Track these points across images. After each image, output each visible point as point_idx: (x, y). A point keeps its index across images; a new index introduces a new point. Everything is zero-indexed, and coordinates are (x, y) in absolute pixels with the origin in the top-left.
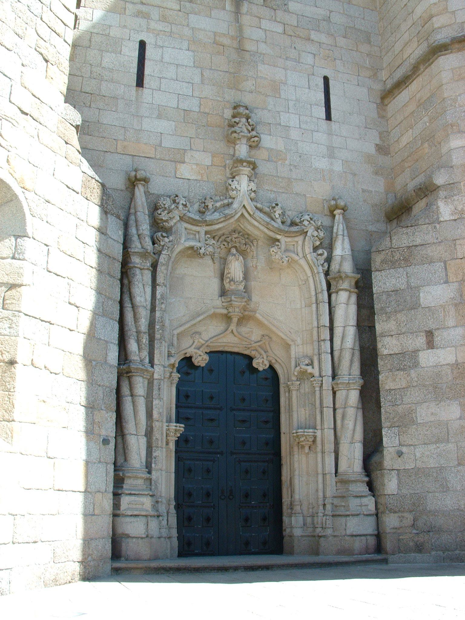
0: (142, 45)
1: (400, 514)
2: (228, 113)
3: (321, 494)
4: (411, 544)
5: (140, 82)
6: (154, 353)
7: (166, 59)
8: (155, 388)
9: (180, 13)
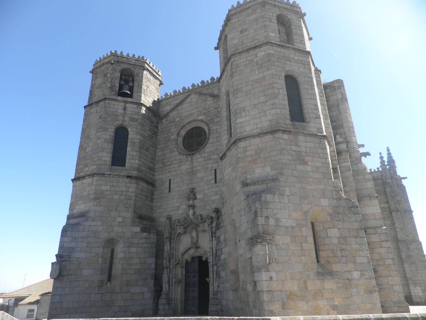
0: (170, 180)
5: (170, 191)
7: (175, 182)
9: (178, 167)
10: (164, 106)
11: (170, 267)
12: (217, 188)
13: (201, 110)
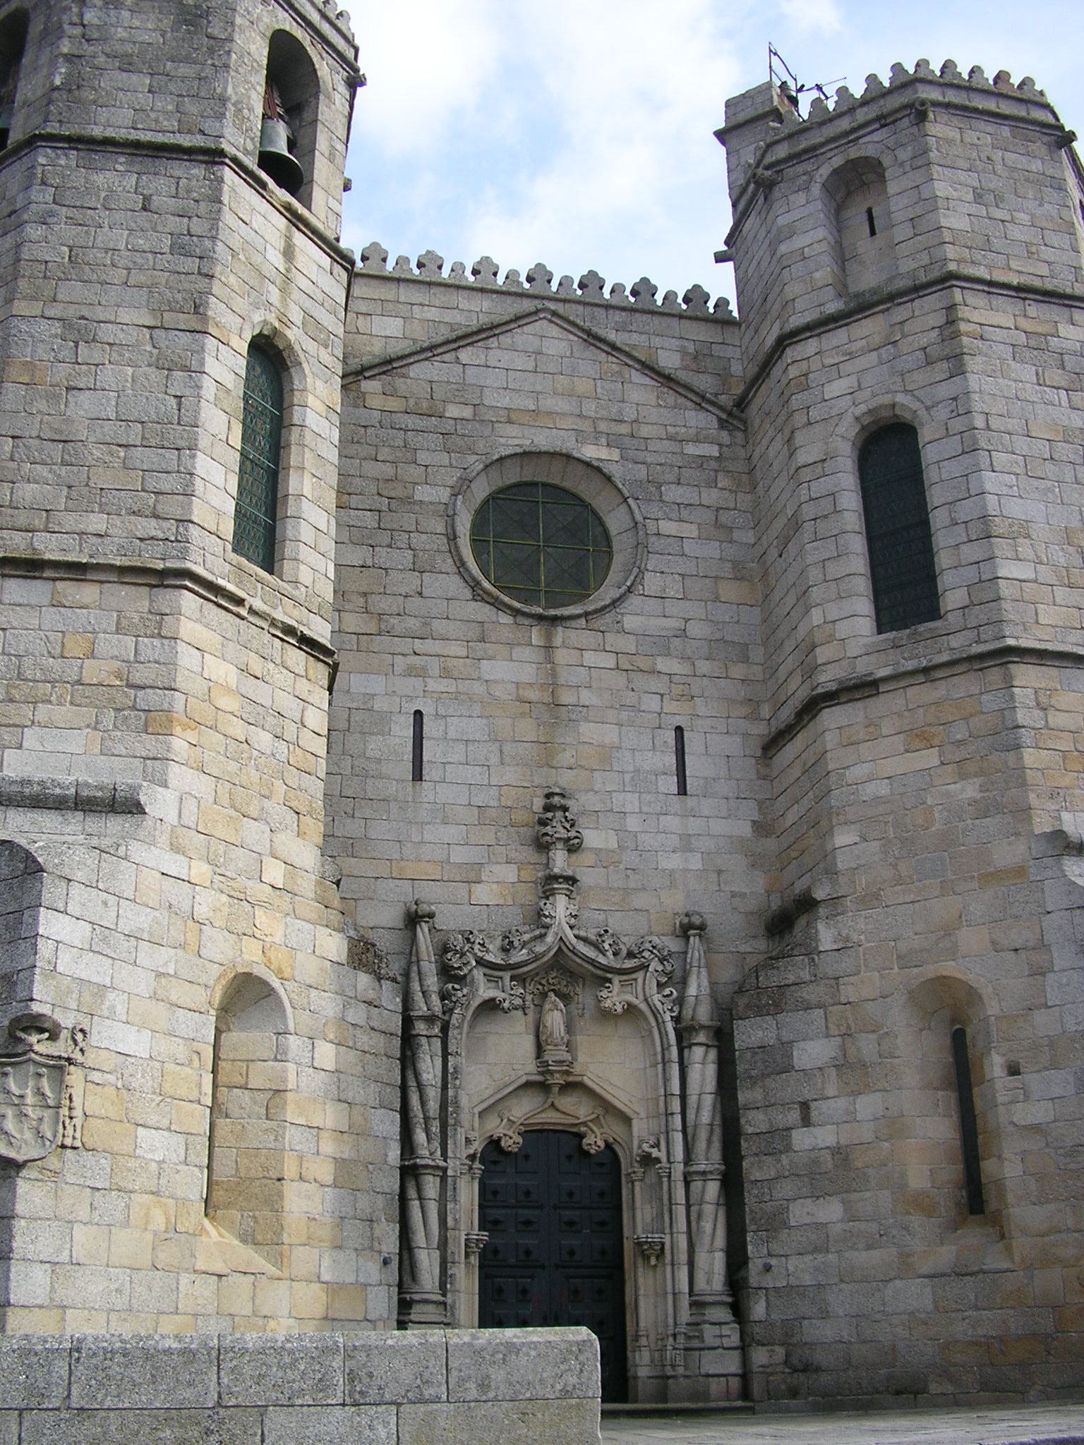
0: (418, 714)
1: (769, 1348)
2: (539, 803)
3: (671, 1321)
4: (783, 1387)
5: (418, 775)
6: (447, 1144)
7: (452, 734)
8: (450, 1187)
10: (364, 310)
11: (445, 1170)
12: (691, 819)
13: (593, 414)
